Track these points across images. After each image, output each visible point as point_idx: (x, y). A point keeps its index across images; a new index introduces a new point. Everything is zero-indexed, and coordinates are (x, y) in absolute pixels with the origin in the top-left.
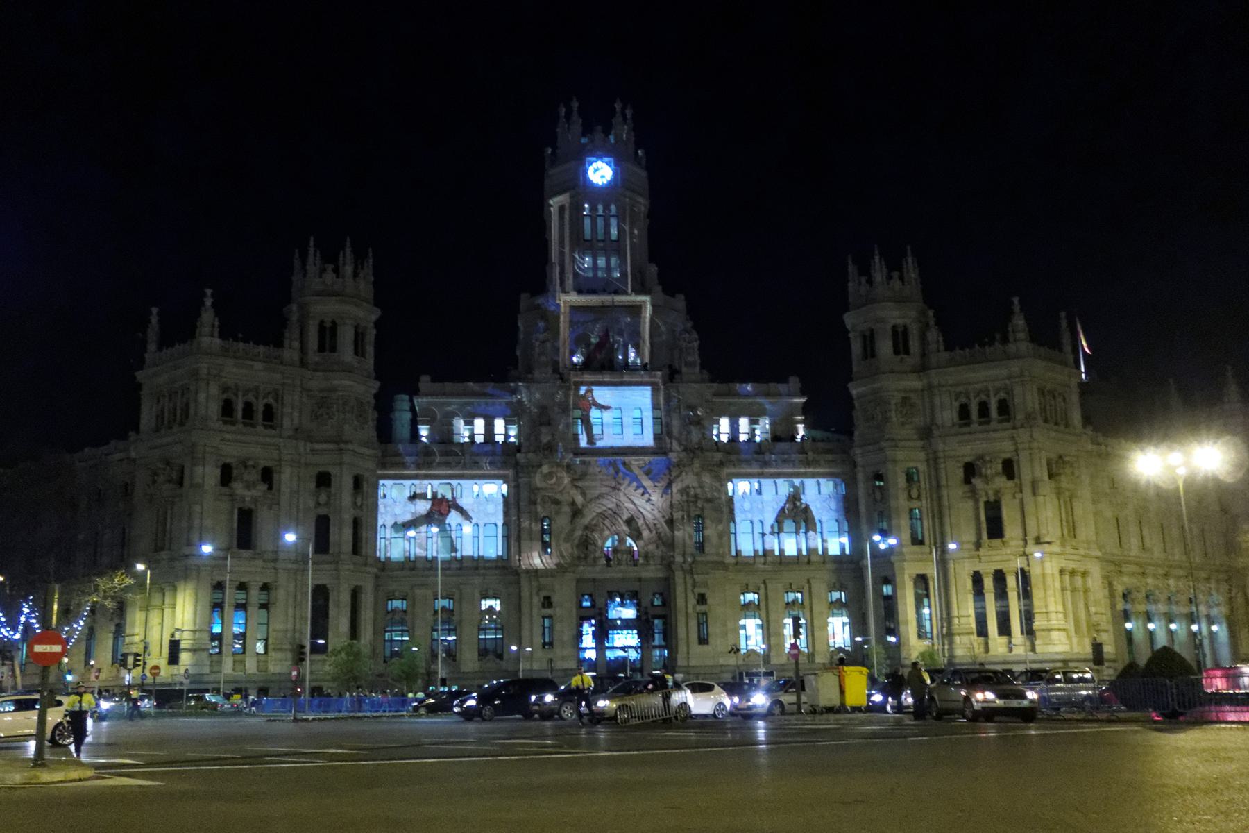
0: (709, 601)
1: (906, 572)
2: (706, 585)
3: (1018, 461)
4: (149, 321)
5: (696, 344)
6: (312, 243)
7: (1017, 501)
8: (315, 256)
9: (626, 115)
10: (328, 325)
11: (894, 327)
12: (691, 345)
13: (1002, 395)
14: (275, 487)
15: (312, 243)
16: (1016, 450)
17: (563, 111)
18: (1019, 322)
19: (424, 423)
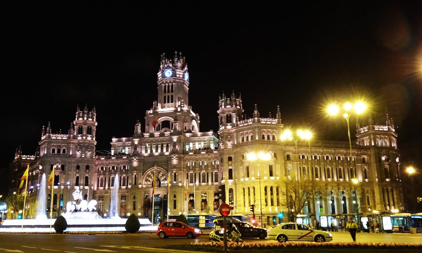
2: (176, 192)
6: (78, 106)
8: (79, 109)
11: (227, 115)
12: (176, 124)
15: (78, 106)
18: (256, 112)
19: (113, 149)
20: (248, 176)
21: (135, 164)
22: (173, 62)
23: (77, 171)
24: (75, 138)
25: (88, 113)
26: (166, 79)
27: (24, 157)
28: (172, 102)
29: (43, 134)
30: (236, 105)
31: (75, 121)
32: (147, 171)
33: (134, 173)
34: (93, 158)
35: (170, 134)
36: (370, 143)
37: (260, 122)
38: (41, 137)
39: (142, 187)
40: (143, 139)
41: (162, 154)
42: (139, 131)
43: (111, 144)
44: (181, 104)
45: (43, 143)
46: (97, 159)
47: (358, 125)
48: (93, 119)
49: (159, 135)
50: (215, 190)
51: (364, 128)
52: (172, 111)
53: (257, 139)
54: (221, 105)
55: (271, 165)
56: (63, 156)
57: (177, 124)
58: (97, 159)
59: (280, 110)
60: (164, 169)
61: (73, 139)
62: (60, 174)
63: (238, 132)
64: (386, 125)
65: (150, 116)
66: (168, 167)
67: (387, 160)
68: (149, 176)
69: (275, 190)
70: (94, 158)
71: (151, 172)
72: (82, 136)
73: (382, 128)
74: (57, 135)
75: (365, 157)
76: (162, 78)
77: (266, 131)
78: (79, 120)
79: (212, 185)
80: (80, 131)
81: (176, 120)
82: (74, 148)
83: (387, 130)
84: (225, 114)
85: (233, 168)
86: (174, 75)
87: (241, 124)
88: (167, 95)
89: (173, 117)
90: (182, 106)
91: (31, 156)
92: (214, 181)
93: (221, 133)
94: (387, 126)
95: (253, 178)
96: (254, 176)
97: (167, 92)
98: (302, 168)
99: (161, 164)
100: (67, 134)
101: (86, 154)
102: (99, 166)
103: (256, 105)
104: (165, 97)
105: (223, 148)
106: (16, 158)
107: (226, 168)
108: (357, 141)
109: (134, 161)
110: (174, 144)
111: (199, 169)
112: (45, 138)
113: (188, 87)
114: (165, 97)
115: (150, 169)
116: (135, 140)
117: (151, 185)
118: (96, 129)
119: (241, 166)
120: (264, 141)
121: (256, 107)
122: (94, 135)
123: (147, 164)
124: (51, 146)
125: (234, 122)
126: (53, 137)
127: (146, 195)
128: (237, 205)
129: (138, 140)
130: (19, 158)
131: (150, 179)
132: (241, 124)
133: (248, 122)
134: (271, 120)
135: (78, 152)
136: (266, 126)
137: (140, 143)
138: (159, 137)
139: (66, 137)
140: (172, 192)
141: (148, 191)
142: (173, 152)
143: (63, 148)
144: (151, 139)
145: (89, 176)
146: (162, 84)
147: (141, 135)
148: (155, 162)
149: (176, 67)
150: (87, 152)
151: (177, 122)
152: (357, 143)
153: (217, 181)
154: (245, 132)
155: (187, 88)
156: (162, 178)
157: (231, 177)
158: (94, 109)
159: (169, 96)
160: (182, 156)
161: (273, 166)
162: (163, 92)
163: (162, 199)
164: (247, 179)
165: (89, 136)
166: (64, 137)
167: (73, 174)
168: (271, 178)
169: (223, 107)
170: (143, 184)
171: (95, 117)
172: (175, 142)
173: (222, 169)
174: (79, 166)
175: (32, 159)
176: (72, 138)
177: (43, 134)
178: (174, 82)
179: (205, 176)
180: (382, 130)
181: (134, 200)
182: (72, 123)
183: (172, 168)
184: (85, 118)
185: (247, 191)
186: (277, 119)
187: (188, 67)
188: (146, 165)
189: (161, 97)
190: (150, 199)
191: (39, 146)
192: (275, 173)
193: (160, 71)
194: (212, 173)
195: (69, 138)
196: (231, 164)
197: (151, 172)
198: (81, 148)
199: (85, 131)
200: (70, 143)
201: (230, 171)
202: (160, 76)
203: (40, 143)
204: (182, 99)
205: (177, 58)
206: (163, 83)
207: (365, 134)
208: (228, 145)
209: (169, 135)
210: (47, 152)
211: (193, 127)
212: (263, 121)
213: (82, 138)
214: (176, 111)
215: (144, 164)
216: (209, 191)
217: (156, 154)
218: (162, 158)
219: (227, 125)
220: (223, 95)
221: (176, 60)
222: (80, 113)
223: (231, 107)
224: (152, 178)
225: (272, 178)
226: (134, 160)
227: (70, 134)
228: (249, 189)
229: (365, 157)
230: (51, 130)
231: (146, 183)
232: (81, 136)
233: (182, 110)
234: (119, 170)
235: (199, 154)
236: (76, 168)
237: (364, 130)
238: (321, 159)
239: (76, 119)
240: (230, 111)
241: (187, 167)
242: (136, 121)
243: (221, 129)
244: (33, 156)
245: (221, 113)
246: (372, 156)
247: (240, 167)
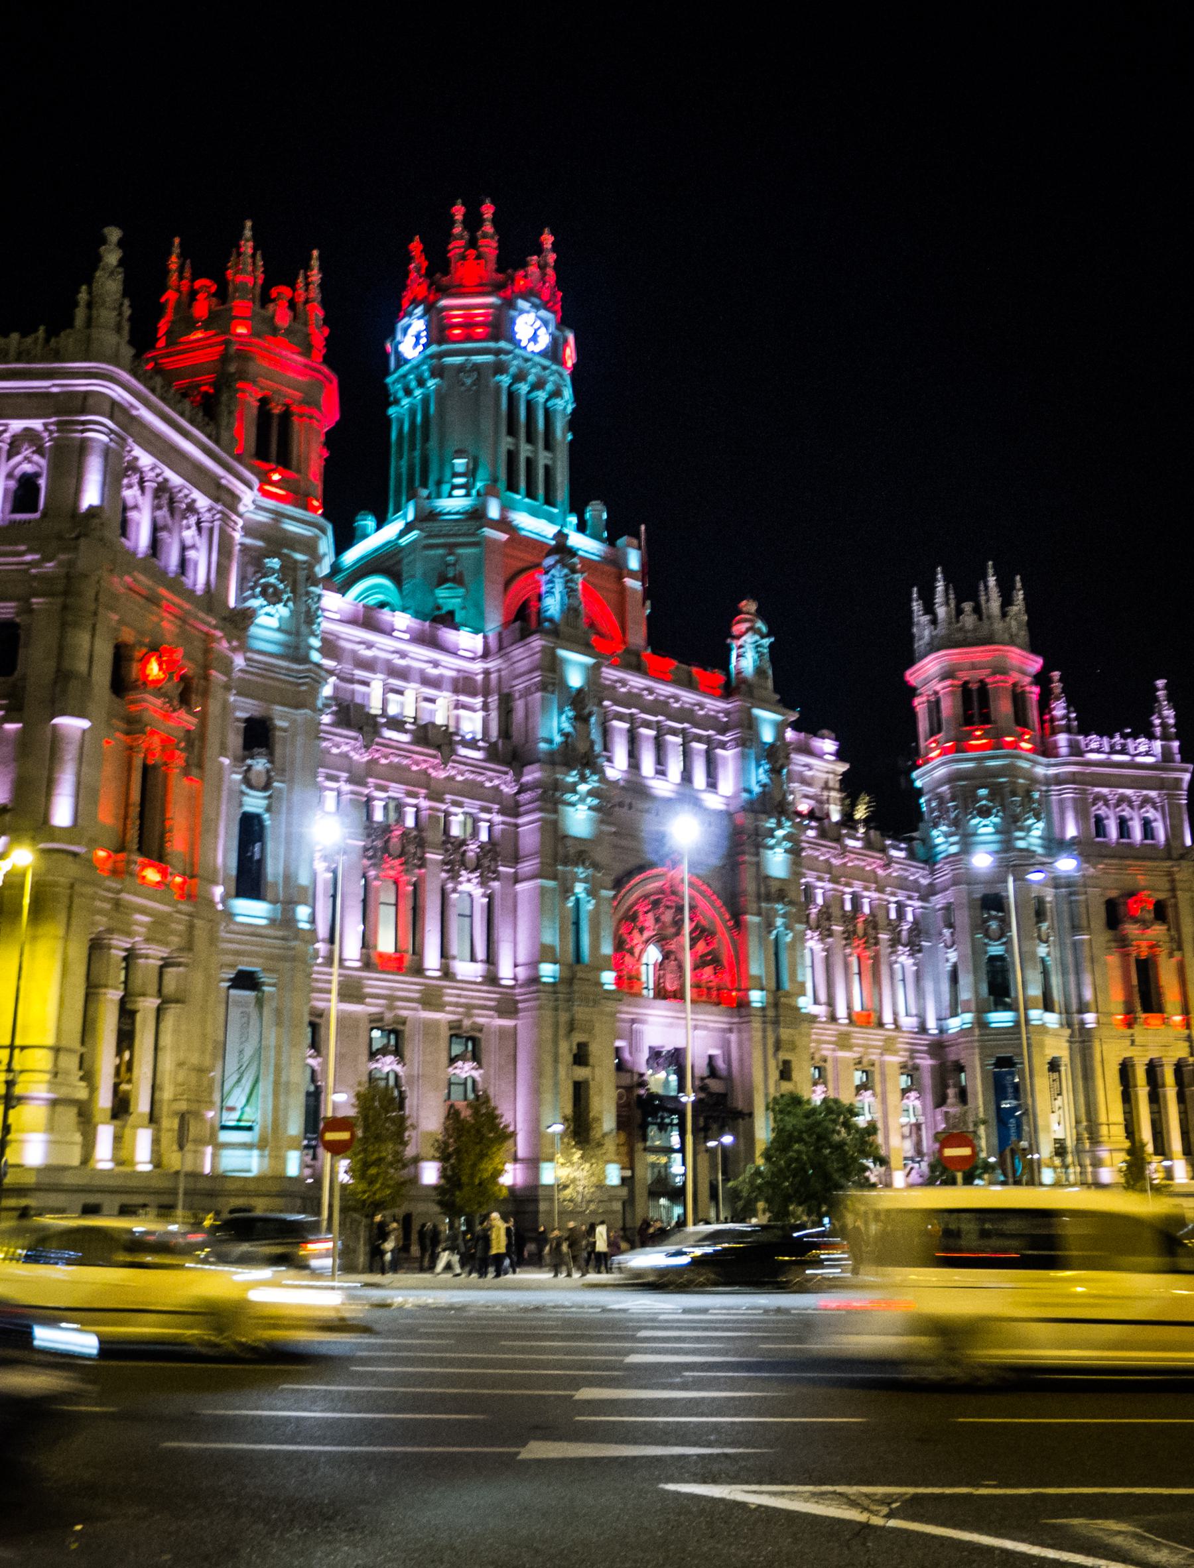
0: (795, 1075)
3: (1176, 906)
5: (766, 642)
16: (1173, 890)
17: (459, 211)
23: (260, 765)
26: (527, 360)
86: (554, 353)
87: (1096, 748)
103: (1160, 683)
104: (512, 456)
109: (574, 798)
114: (512, 456)
132: (1092, 751)
133: (1132, 751)
135: (270, 609)
140: (771, 1051)
141: (633, 1021)
159: (530, 462)
181: (581, 1073)
183: (768, 898)
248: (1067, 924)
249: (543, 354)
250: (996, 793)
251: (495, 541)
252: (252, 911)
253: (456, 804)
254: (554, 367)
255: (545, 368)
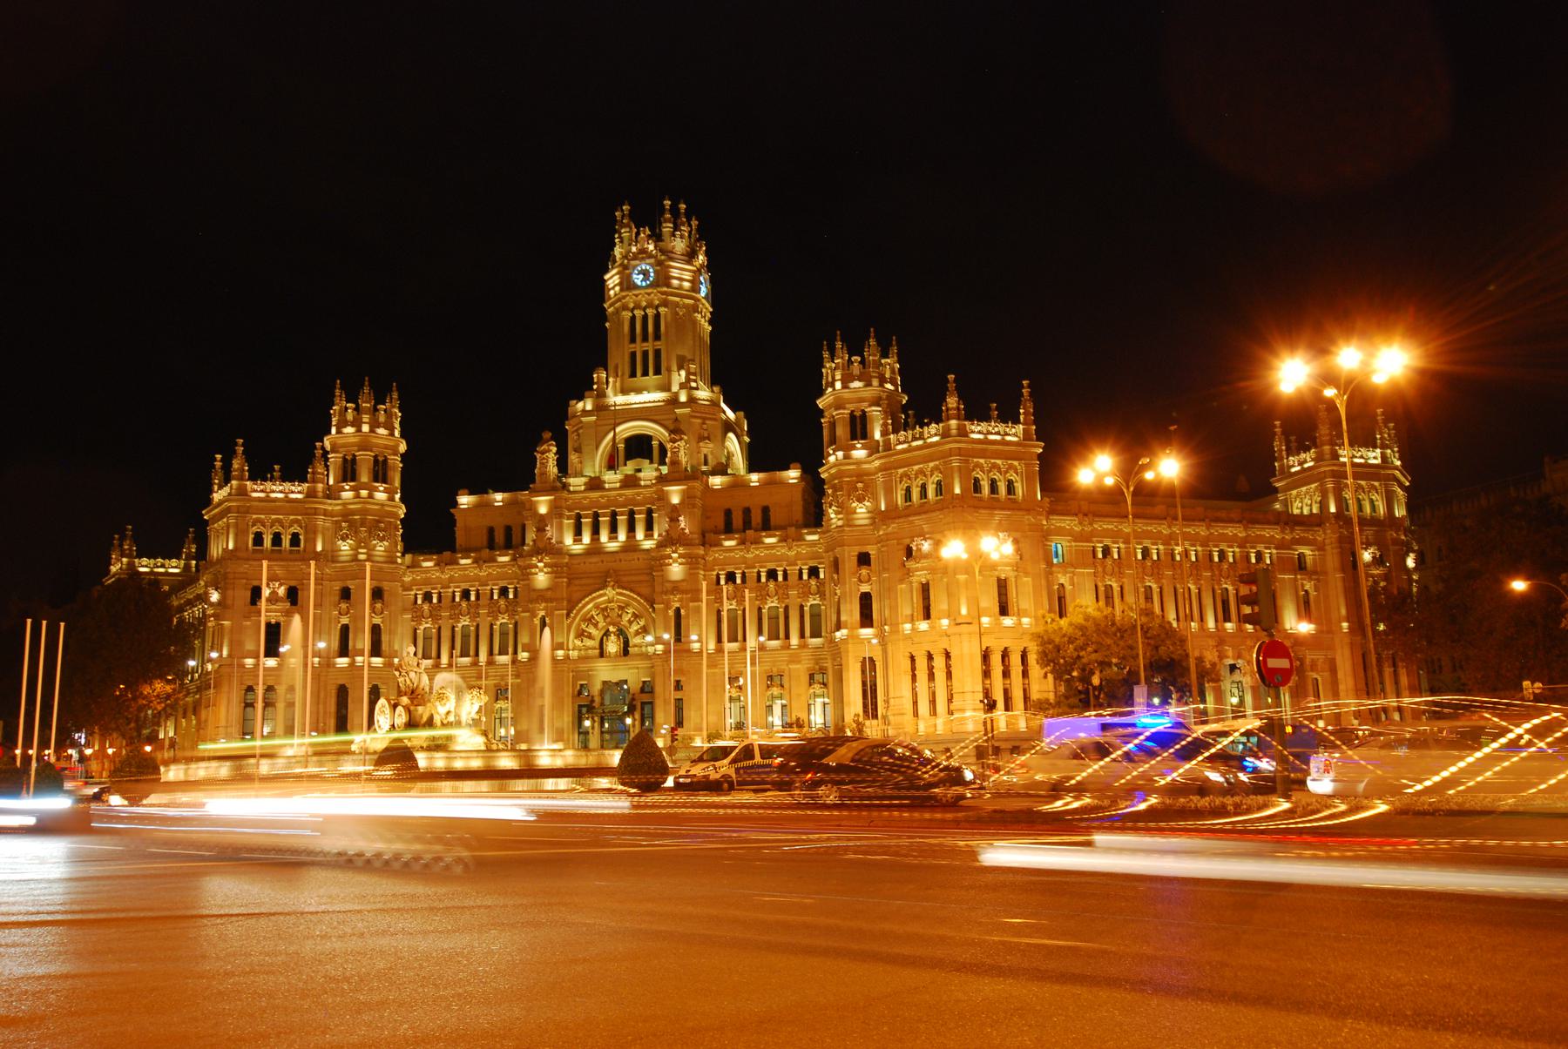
1: (850, 654)
4: (214, 466)
6: (338, 386)
7: (945, 580)
9: (679, 209)
10: (349, 458)
11: (852, 415)
12: (676, 445)
13: (935, 478)
14: (299, 603)
15: (338, 386)
18: (952, 401)
20: (927, 616)
21: (541, 579)
22: (657, 237)
23: (344, 606)
24: (332, 494)
25: (376, 410)
26: (637, 296)
27: (144, 563)
28: (657, 372)
29: (216, 481)
30: (882, 380)
31: (329, 437)
32: (583, 602)
33: (540, 610)
34: (396, 563)
35: (656, 478)
36: (1323, 505)
37: (967, 436)
38: (211, 492)
39: (567, 657)
40: (565, 494)
41: (631, 547)
42: (553, 469)
43: (453, 515)
44: (688, 380)
45: (222, 511)
46: (408, 567)
47: (1281, 446)
48: (391, 430)
49: (621, 481)
50: (811, 665)
51: (1303, 456)
52: (659, 401)
53: (957, 491)
54: (830, 379)
55: (1003, 576)
56: (292, 556)
57: (682, 443)
58: (408, 567)
59: (1031, 394)
60: (639, 594)
61: (324, 497)
62: (282, 619)
63: (890, 469)
64: (1375, 447)
65: (583, 419)
66: (654, 591)
67: (1378, 561)
68: (589, 620)
69: (1015, 660)
70: (399, 561)
71: (597, 607)
72: (355, 489)
73: (1362, 457)
74: (269, 485)
75: (1307, 551)
76: (621, 290)
77: (985, 465)
78: (342, 435)
79: (803, 646)
80: (349, 471)
81: (676, 431)
82: (328, 529)
83: (1378, 461)
84: (844, 409)
85: (874, 589)
87: (902, 442)
88: (639, 347)
89: (662, 422)
90: (694, 385)
91: (167, 562)
92: (807, 633)
93: (831, 475)
94: (1378, 451)
95: (945, 622)
96: (948, 617)
97: (638, 339)
98: (1102, 589)
99: (629, 578)
100: (303, 480)
101: (371, 549)
102: (417, 590)
103: (951, 377)
104: (633, 355)
105: (840, 523)
106: (114, 569)
107: (850, 589)
108: (1276, 500)
110: (674, 514)
111: (758, 593)
112: (226, 494)
113: (711, 322)
114: (633, 355)
115: (594, 595)
116: (538, 501)
117: (598, 651)
118: (401, 465)
119: (901, 581)
120: (981, 499)
121: (951, 386)
122: (397, 483)
123: (583, 582)
124: (250, 524)
125: (877, 435)
126: (257, 491)
127: (582, 685)
128: (888, 714)
129: (550, 501)
130: (127, 569)
131: (592, 630)
132: (900, 443)
133: (926, 435)
134: (1001, 427)
136: (985, 449)
137: (556, 510)
138: (621, 488)
139: (299, 492)
141: (588, 671)
142: (669, 541)
143: (292, 530)
144: (595, 495)
145: (382, 622)
146: (624, 313)
147: (559, 484)
148: (608, 571)
149: (669, 254)
150: (374, 542)
151: (681, 439)
152: (1278, 506)
153: (819, 636)
154: (916, 467)
155: (707, 324)
156: (635, 627)
157: (866, 619)
158: (395, 395)
159: (645, 354)
160: (701, 551)
161: (1009, 583)
162: (627, 338)
163: (636, 696)
164: (923, 626)
165: (381, 489)
166: (292, 492)
167: (330, 619)
168: (1004, 622)
169: (838, 385)
170: (571, 647)
171: (397, 425)
172: (674, 505)
173: (836, 594)
174: (350, 589)
175: (171, 570)
176: (320, 494)
177: (216, 481)
178: (665, 303)
179: (777, 618)
180: (1362, 461)
182: (318, 444)
184: (366, 428)
185: (922, 664)
186: (1021, 426)
187: (707, 254)
188: (577, 582)
189: (619, 353)
190: (593, 697)
191: (206, 523)
192: (1018, 606)
193: (613, 268)
194: (802, 607)
195: (311, 494)
196: (867, 577)
197: (597, 607)
198: (353, 526)
199: (367, 471)
200: (316, 512)
201: (866, 600)
202: (615, 286)
203: (206, 514)
204: (693, 361)
205: (670, 222)
206: (625, 307)
207: (1305, 478)
208: (855, 513)
209: (654, 482)
210: (236, 542)
211: (729, 456)
212: (977, 431)
213: (358, 496)
214: (673, 402)
215: (570, 580)
216: (791, 666)
217: (614, 546)
218: (634, 560)
219: (854, 448)
220: (839, 345)
221: (667, 228)
222: (346, 409)
223: (866, 386)
224: (601, 625)
225: (1008, 621)
226: (537, 567)
227: (314, 481)
228: (930, 657)
229: (1307, 551)
230: (247, 468)
231: (578, 643)
232: (351, 486)
233: (692, 400)
234: (484, 601)
235: (756, 543)
236: (337, 598)
237: (1301, 464)
238: (1162, 557)
239: (334, 430)
240: (861, 400)
241: (715, 590)
242: (542, 437)
243: (832, 459)
244: (174, 562)
245: (830, 406)
246: (1328, 548)
247: (899, 586)
248: (881, 568)
249: (652, 285)
250: (836, 489)
251: (589, 422)
252: (343, 662)
253: (494, 585)
254: (655, 291)
255: (649, 294)
